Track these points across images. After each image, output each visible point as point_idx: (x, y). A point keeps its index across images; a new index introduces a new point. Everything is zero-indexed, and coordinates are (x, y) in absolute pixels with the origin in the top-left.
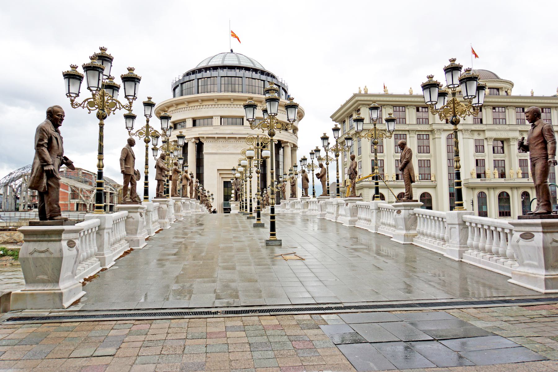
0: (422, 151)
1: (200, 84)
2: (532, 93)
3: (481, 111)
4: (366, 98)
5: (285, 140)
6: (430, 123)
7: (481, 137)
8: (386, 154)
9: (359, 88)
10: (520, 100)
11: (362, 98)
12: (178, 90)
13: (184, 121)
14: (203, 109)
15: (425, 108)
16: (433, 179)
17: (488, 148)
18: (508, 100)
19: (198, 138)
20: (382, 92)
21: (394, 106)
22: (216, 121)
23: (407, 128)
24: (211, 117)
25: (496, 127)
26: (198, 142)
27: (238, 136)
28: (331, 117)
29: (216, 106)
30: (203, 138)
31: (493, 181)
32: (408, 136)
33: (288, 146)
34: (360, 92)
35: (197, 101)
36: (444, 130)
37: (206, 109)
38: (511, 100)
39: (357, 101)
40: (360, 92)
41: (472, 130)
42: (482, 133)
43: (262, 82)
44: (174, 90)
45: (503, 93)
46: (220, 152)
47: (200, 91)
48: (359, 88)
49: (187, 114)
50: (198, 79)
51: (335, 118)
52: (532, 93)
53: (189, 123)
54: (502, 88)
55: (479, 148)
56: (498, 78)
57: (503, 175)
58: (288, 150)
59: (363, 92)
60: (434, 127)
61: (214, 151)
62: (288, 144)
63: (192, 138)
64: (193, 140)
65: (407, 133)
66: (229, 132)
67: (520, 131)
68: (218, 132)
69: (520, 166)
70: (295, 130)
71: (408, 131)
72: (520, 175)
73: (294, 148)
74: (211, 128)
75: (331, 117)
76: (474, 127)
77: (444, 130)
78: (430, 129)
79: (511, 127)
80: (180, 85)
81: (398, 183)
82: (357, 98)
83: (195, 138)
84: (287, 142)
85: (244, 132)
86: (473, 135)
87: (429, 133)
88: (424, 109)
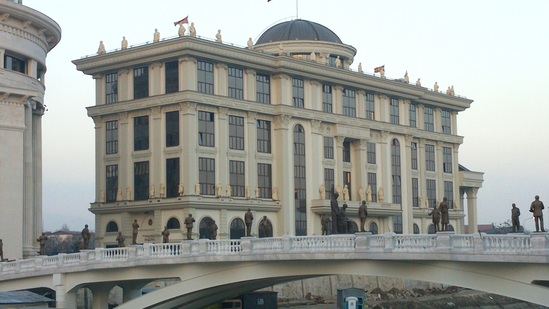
6: (274, 102)
8: (218, 150)
20: (213, 38)
21: (230, 66)
32: (246, 120)
36: (293, 118)
60: (282, 110)
65: (245, 115)
77: (293, 118)
78: (274, 112)
79: (361, 123)
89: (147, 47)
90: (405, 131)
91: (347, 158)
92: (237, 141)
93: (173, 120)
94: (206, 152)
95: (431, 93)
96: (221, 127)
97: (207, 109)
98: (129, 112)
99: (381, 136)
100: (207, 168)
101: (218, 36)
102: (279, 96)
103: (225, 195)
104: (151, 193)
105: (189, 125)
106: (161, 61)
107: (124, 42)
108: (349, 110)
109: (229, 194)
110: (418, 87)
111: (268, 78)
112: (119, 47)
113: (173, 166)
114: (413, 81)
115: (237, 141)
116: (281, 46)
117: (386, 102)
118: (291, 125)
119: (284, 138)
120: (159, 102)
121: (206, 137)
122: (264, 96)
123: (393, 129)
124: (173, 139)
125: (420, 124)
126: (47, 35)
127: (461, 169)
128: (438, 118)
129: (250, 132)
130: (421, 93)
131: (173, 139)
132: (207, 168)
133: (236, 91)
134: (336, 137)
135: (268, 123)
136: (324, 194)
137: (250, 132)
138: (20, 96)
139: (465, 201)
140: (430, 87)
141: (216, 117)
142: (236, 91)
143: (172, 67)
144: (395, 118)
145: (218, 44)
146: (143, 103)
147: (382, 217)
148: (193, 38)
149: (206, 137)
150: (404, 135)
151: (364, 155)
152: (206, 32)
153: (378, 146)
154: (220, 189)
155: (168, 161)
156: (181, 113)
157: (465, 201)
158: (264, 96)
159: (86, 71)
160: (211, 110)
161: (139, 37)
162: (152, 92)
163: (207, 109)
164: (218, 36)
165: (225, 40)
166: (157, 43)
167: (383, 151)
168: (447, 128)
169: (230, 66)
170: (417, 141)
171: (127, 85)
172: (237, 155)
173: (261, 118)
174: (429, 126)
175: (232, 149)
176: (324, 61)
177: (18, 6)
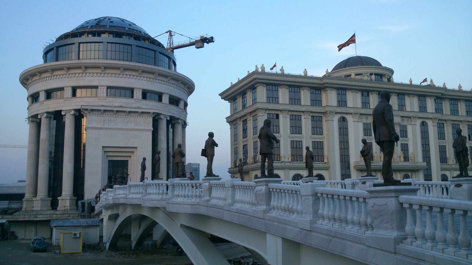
0: (295, 132)
1: (81, 49)
2: (411, 81)
3: (368, 96)
4: (264, 77)
5: (177, 116)
6: (324, 104)
8: (282, 135)
9: (256, 66)
10: (402, 88)
11: (261, 77)
12: (49, 55)
13: (62, 89)
14: (86, 78)
15: (318, 90)
16: (326, 161)
18: (390, 87)
19: (78, 111)
21: (290, 86)
22: (102, 92)
24: (96, 87)
26: (77, 114)
27: (128, 110)
28: (220, 95)
30: (87, 110)
31: (401, 164)
32: (303, 117)
33: (179, 123)
35: (80, 68)
36: (337, 113)
37: (90, 77)
39: (255, 79)
41: (361, 114)
43: (153, 52)
44: (46, 53)
45: (385, 80)
46: (107, 126)
47: (81, 57)
48: (256, 66)
49: (65, 81)
50: (80, 43)
51: (224, 96)
52: (411, 81)
53: (68, 93)
54: (384, 75)
56: (380, 65)
57: (406, 158)
58: (179, 128)
59: (260, 70)
60: (327, 109)
61: (98, 126)
62: (180, 121)
63: (71, 110)
64: (73, 112)
65: (302, 114)
66: (117, 104)
67: (401, 117)
68: (104, 104)
69: (402, 150)
70: (186, 105)
71: (303, 112)
72: (402, 159)
73: (185, 124)
74: (96, 99)
75: (220, 95)
76: (363, 111)
78: (323, 111)
80: (55, 49)
81: (294, 164)
82: (255, 76)
83: (74, 110)
84: (178, 119)
87: (322, 115)
88: (317, 92)
97: (273, 112)
99: (411, 120)
103: (287, 161)
109: (290, 160)
119: (331, 127)
122: (316, 102)
129: (306, 123)
137: (306, 123)
141: (281, 116)
150: (431, 118)
154: (283, 158)
158: (316, 102)
160: (277, 113)
162: (248, 105)
163: (273, 112)
165: (286, 72)
173: (314, 115)
175: (293, 134)
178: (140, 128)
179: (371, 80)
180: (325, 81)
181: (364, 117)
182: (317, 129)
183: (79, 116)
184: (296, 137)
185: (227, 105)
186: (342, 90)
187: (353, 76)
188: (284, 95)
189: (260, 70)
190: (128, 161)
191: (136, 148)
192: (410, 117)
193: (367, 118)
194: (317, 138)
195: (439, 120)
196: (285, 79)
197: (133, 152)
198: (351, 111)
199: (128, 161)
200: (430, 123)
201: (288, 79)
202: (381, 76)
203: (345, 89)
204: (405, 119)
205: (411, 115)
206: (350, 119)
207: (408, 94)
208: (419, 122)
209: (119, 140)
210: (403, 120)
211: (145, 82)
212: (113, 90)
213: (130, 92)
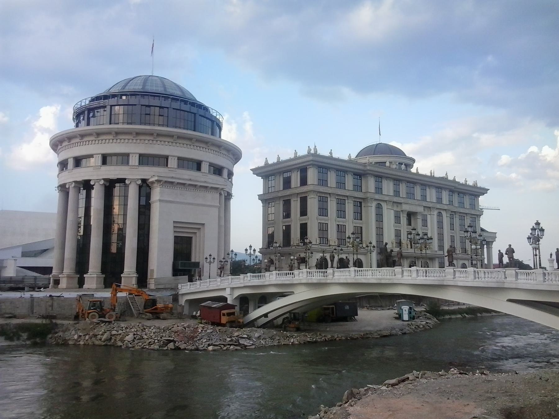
7: (399, 209)
17: (404, 219)
19: (144, 181)
23: (348, 194)
24: (167, 158)
25: (410, 201)
29: (174, 144)
34: (309, 150)
36: (376, 200)
38: (411, 176)
40: (309, 150)
41: (394, 202)
42: (399, 205)
46: (178, 200)
55: (397, 219)
60: (369, 195)
66: (186, 177)
76: (396, 199)
77: (376, 200)
85: (203, 180)
86: (393, 205)
89: (291, 160)
90: (446, 207)
91: (409, 224)
92: (341, 213)
93: (304, 201)
94: (323, 219)
95: (462, 184)
96: (332, 206)
98: (280, 197)
100: (323, 229)
101: (331, 153)
102: (367, 187)
104: (292, 243)
105: (313, 204)
106: (298, 168)
107: (279, 158)
108: (411, 195)
110: (454, 181)
111: (360, 177)
112: (276, 161)
113: (304, 228)
114: (451, 178)
115: (341, 213)
116: (368, 158)
117: (434, 191)
118: (374, 204)
119: (370, 212)
120: (297, 191)
121: (323, 211)
122: (358, 187)
123: (438, 206)
124: (304, 212)
125: (456, 204)
126: (234, 155)
127: (482, 230)
128: (467, 200)
129: (349, 208)
130: (457, 185)
131: (304, 212)
132: (323, 229)
133: (341, 184)
134: (402, 211)
135: (361, 203)
136: (394, 245)
137: (349, 208)
138: (216, 189)
139: (485, 250)
140: (462, 181)
142: (341, 184)
143: (303, 171)
144: (439, 200)
145: (331, 158)
146: (288, 192)
147: (432, 259)
148: (316, 155)
149: (323, 211)
151: (420, 222)
152: (324, 151)
153: (429, 217)
155: (301, 225)
156: (308, 197)
157: (485, 250)
159: (258, 175)
161: (287, 154)
162: (293, 185)
164: (331, 153)
165: (335, 155)
166: (296, 158)
167: (432, 220)
168: (474, 205)
169: (338, 170)
170: (453, 214)
171: (279, 183)
172: (341, 221)
174: (462, 204)
176: (394, 166)
177: (219, 139)
178: (209, 203)
179: (400, 169)
180: (368, 168)
181: (395, 205)
182: (359, 215)
183: (145, 187)
184: (341, 221)
185: (260, 181)
186: (379, 177)
187: (388, 164)
188: (332, 178)
189: (312, 152)
190: (191, 238)
191: (203, 224)
192: (430, 208)
193: (398, 206)
194: (358, 223)
195: (452, 211)
196: (333, 162)
197: (199, 229)
198: (387, 198)
199: (191, 238)
200: (444, 213)
201: (338, 163)
202: (406, 165)
203: (381, 177)
204: (426, 209)
205: (431, 205)
206: (384, 205)
207: (430, 186)
208: (435, 213)
209: (189, 216)
210: (424, 210)
211: (212, 155)
212: (183, 162)
213: (198, 165)
